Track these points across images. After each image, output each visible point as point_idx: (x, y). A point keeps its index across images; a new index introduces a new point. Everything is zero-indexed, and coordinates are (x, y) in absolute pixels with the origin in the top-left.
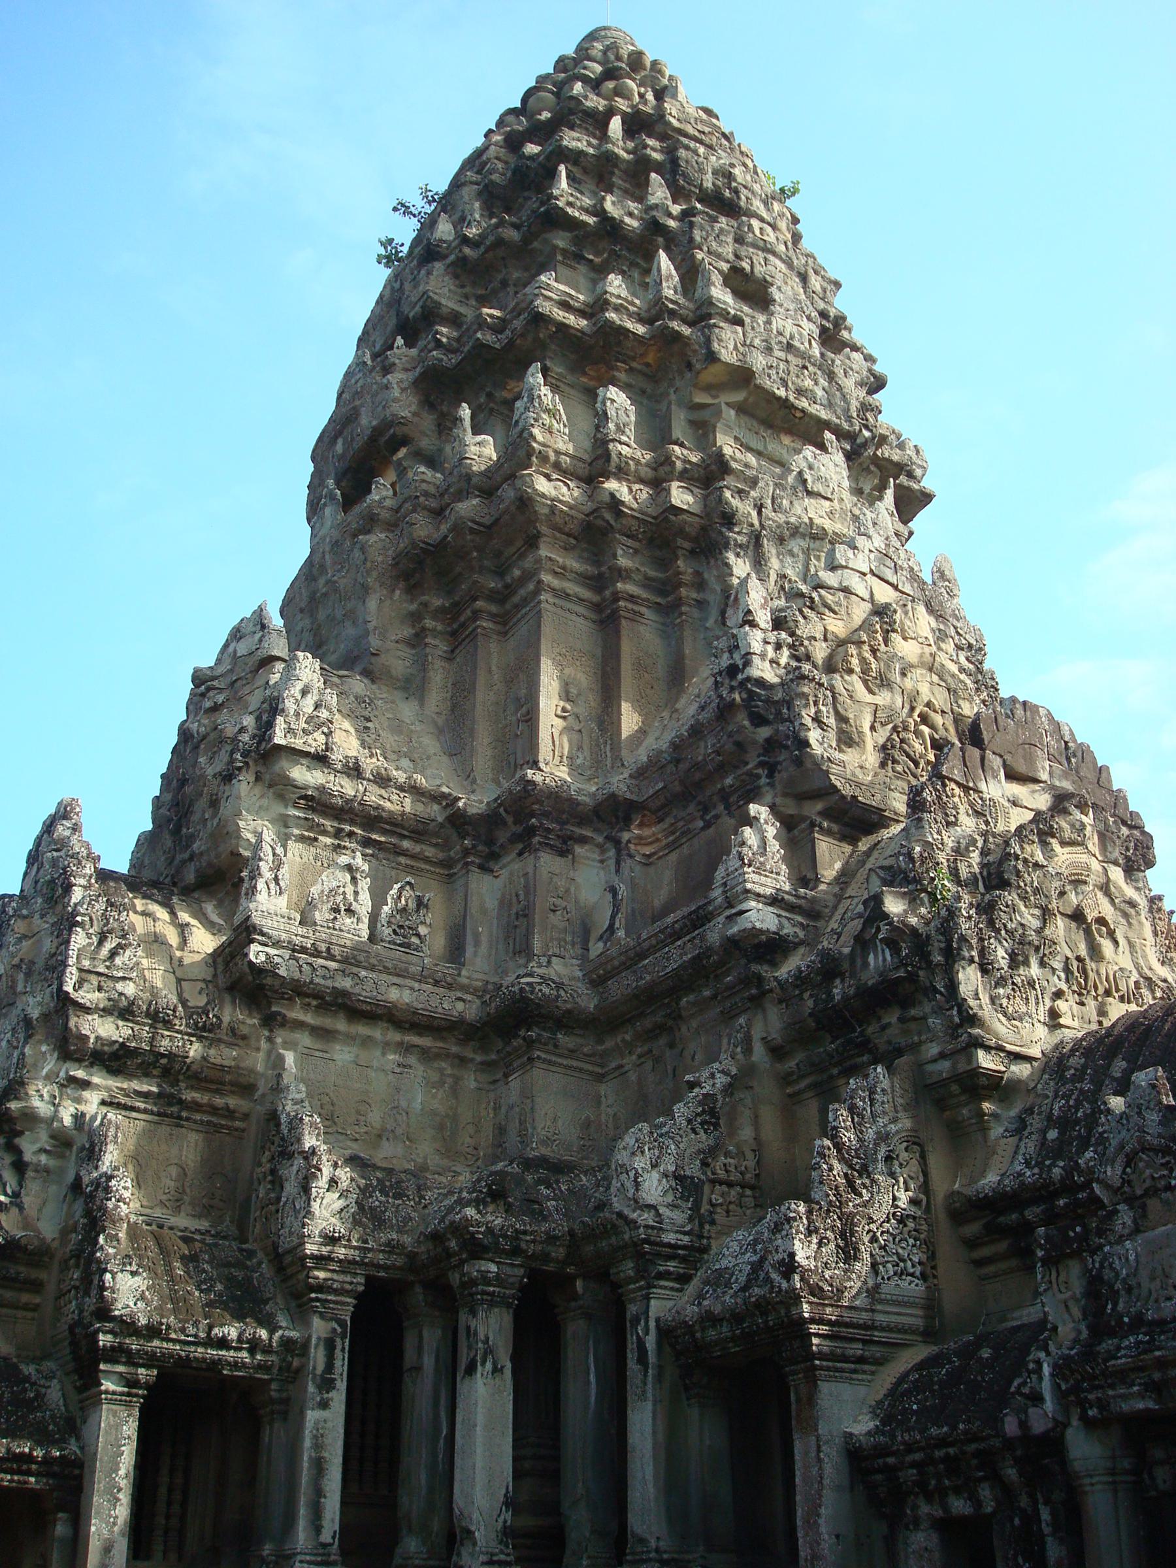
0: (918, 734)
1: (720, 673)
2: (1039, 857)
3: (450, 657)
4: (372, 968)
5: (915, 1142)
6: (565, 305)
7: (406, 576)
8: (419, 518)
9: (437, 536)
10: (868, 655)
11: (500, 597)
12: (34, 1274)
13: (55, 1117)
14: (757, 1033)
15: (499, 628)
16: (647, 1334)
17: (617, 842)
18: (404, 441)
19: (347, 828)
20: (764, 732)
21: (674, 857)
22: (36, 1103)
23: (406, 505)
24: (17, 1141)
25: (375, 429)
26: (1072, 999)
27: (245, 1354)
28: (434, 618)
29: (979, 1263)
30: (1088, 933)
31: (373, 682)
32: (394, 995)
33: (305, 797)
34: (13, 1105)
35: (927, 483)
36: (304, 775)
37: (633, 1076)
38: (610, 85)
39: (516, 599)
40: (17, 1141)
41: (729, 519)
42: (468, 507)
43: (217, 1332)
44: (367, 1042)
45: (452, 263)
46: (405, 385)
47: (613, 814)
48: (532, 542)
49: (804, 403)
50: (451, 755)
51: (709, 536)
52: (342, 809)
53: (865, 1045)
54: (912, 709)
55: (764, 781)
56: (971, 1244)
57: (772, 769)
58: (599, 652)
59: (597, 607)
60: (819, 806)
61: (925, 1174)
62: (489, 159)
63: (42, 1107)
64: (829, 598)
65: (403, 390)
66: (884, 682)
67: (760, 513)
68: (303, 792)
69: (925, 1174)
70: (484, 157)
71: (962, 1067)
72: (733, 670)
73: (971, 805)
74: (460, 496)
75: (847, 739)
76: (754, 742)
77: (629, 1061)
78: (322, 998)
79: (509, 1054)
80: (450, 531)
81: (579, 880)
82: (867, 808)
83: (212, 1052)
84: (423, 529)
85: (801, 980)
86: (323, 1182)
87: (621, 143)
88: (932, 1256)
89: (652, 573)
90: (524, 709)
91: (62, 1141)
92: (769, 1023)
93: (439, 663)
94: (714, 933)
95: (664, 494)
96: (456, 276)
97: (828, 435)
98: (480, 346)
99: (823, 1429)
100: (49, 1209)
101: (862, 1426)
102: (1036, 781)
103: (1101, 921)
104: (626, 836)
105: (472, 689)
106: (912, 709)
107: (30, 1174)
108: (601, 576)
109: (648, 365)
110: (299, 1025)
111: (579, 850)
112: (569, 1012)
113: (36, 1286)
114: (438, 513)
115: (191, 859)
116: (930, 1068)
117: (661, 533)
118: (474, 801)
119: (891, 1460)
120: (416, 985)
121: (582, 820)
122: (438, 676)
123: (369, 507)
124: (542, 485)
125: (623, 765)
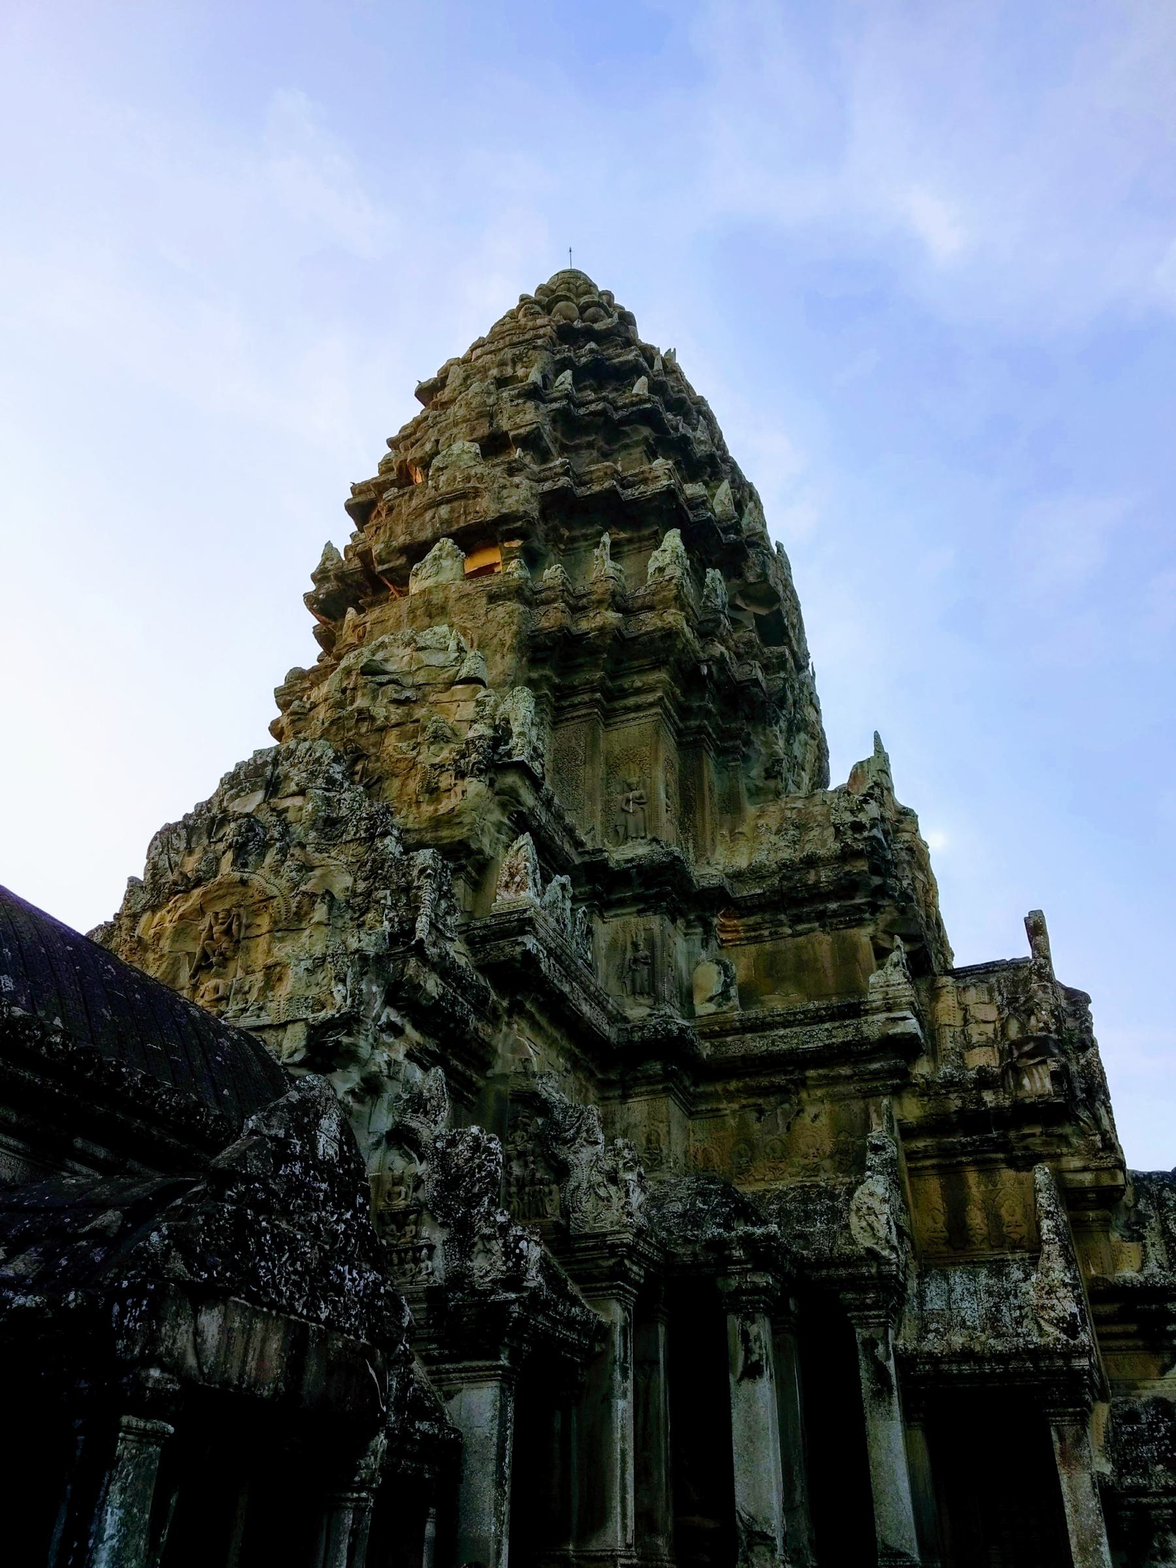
16: (888, 1358)
20: (877, 881)
21: (753, 949)
22: (362, 1043)
23: (549, 593)
33: (520, 813)
37: (732, 1122)
39: (631, 701)
47: (715, 900)
53: (1003, 1146)
57: (875, 909)
59: (679, 733)
68: (521, 808)
77: (727, 1107)
92: (911, 1109)
94: (874, 1026)
104: (715, 921)
116: (1069, 1176)
125: (708, 863)
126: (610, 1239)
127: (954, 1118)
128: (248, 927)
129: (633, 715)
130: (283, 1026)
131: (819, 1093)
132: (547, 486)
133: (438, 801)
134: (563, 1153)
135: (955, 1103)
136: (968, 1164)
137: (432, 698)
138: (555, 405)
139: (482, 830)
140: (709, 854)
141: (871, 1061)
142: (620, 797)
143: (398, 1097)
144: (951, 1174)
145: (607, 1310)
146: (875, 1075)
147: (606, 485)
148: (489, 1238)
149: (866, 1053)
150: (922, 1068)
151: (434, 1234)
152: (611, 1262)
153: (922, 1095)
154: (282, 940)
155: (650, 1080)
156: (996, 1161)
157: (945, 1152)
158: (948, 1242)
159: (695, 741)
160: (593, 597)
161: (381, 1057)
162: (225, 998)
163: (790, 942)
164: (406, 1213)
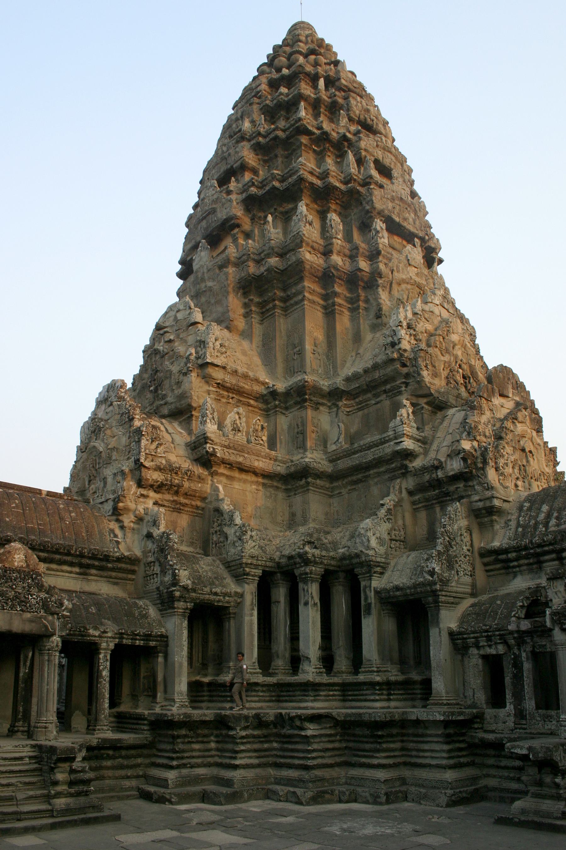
0: (458, 372)
1: (387, 344)
2: (512, 428)
3: (261, 322)
4: (248, 453)
5: (469, 530)
6: (311, 173)
7: (243, 288)
8: (251, 264)
9: (258, 273)
10: (442, 340)
11: (285, 300)
12: (133, 568)
13: (136, 509)
14: (404, 485)
15: (283, 313)
17: (337, 406)
18: (238, 226)
19: (231, 395)
20: (405, 370)
21: (360, 413)
22: (130, 504)
24: (121, 518)
25: (225, 220)
26: (521, 479)
27: (222, 598)
28: (255, 306)
29: (487, 571)
30: (526, 456)
31: (230, 332)
32: (256, 464)
34: (121, 505)
35: (441, 255)
36: (218, 375)
38: (313, 57)
39: (292, 302)
40: (121, 518)
41: (380, 275)
42: (273, 261)
43: (214, 590)
44: (245, 481)
45: (254, 144)
46: (238, 201)
48: (301, 279)
49: (405, 224)
50: (265, 365)
51: (372, 282)
52: (230, 388)
54: (456, 362)
55: (403, 389)
56: (485, 565)
57: (407, 384)
58: (325, 326)
59: (325, 308)
60: (425, 400)
61: (472, 540)
62: (261, 91)
63: (132, 506)
64: (426, 316)
65: (237, 203)
66: (447, 351)
67: (392, 273)
69: (472, 540)
70: (258, 89)
71: (488, 504)
72: (393, 345)
73: (488, 406)
74: (268, 256)
75: (435, 375)
76: (401, 374)
78: (231, 465)
79: (297, 487)
80: (266, 271)
81: (322, 420)
82: (441, 402)
83: (192, 485)
84: (252, 268)
85: (424, 469)
86: (248, 537)
87: (324, 92)
88: (474, 569)
89: (348, 295)
90: (297, 349)
91: (140, 520)
92: (410, 483)
93: (257, 325)
94: (388, 449)
95: (355, 263)
96: (255, 150)
97: (416, 240)
98: (274, 188)
99: (441, 626)
100: (136, 542)
101: (454, 626)
102: (508, 397)
103: (530, 452)
104: (340, 404)
105: (274, 338)
106: (456, 362)
107: (127, 530)
108: (327, 294)
109: (343, 202)
110: (223, 474)
111: (321, 408)
112: (322, 472)
113: (133, 572)
114: (258, 262)
115: (166, 404)
116: (474, 504)
117: (353, 280)
118: (281, 386)
119: (465, 636)
120: (264, 460)
121: (323, 396)
122: (258, 329)
123: (227, 256)
124: (308, 256)
126: (238, 562)
127: (427, 484)
128: (99, 463)
129: (295, 307)
130: (107, 501)
131: (376, 480)
132: (244, 195)
133: (180, 387)
134: (226, 529)
135: (427, 477)
136: (436, 503)
137: (181, 336)
138: (252, 143)
139: (198, 397)
140: (339, 369)
141: (392, 463)
142: (292, 352)
143: (148, 521)
144: (429, 508)
145: (243, 587)
146: (394, 470)
147: (271, 185)
148: (168, 570)
149: (391, 459)
150: (417, 463)
151: (157, 569)
152: (242, 569)
153: (415, 475)
154: (106, 468)
155: (302, 487)
156: (446, 501)
157: (427, 500)
158: (427, 539)
159: (332, 310)
160: (265, 253)
161: (141, 508)
162: (95, 492)
163: (375, 407)
164: (151, 563)
